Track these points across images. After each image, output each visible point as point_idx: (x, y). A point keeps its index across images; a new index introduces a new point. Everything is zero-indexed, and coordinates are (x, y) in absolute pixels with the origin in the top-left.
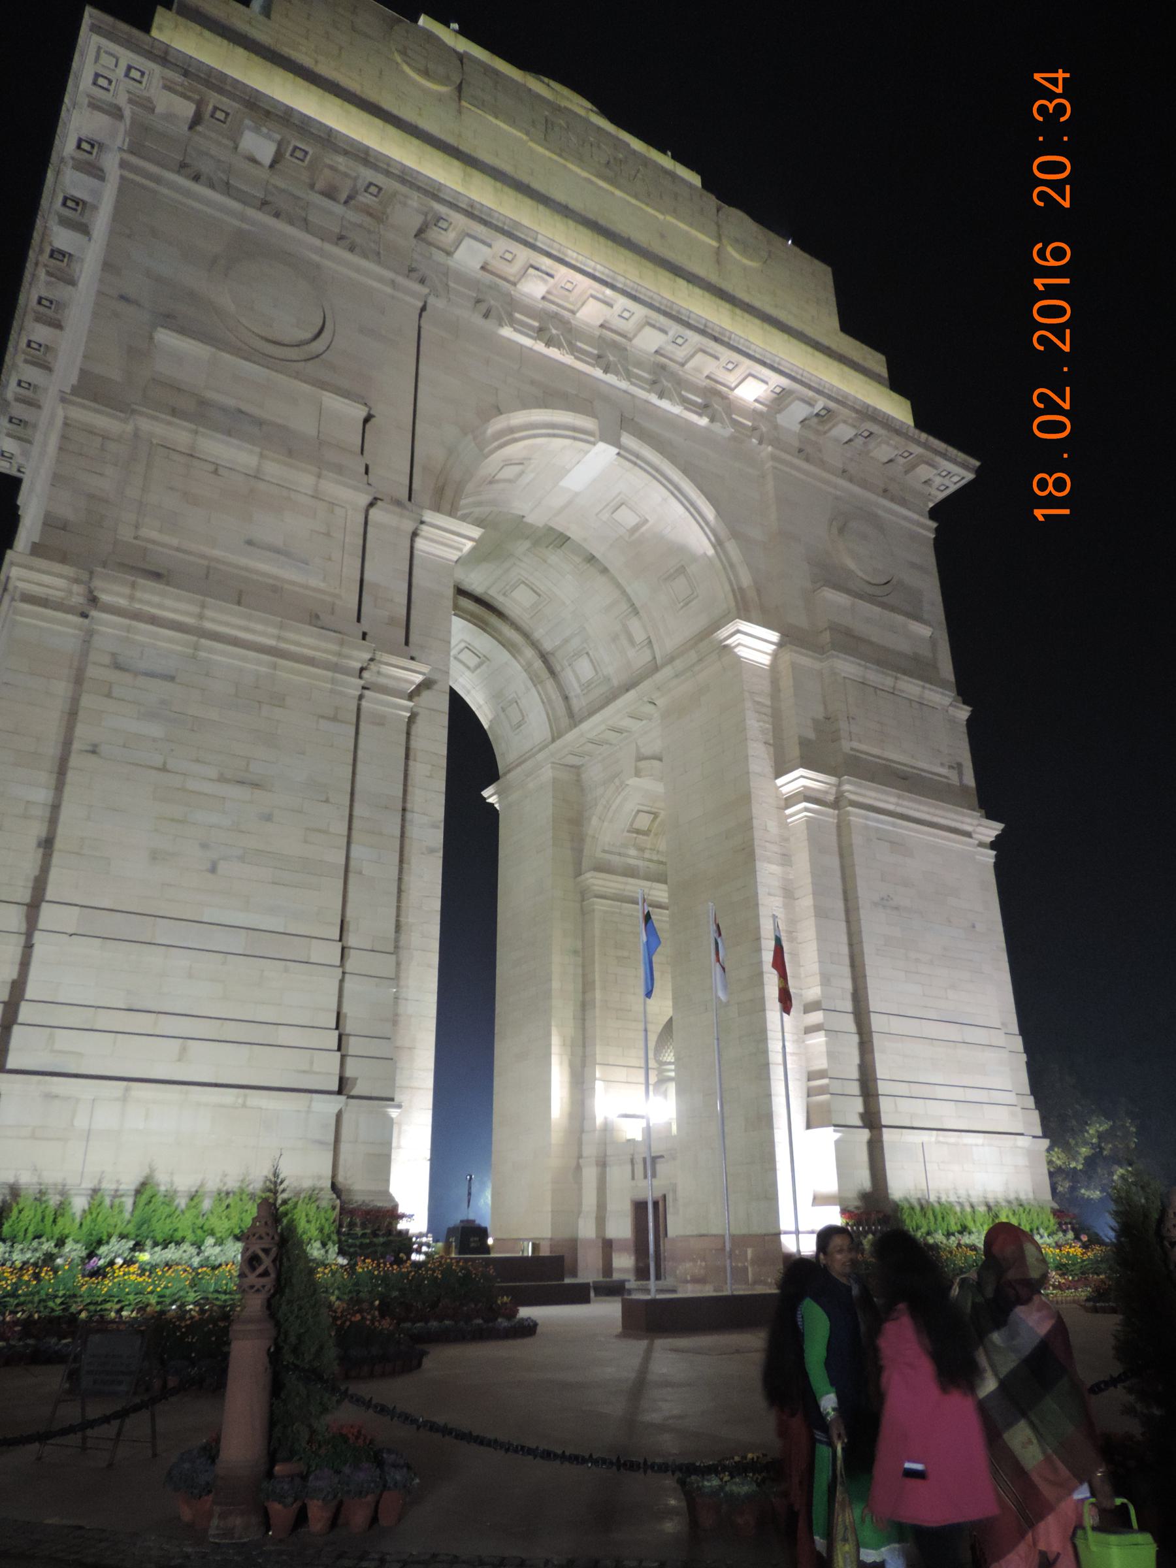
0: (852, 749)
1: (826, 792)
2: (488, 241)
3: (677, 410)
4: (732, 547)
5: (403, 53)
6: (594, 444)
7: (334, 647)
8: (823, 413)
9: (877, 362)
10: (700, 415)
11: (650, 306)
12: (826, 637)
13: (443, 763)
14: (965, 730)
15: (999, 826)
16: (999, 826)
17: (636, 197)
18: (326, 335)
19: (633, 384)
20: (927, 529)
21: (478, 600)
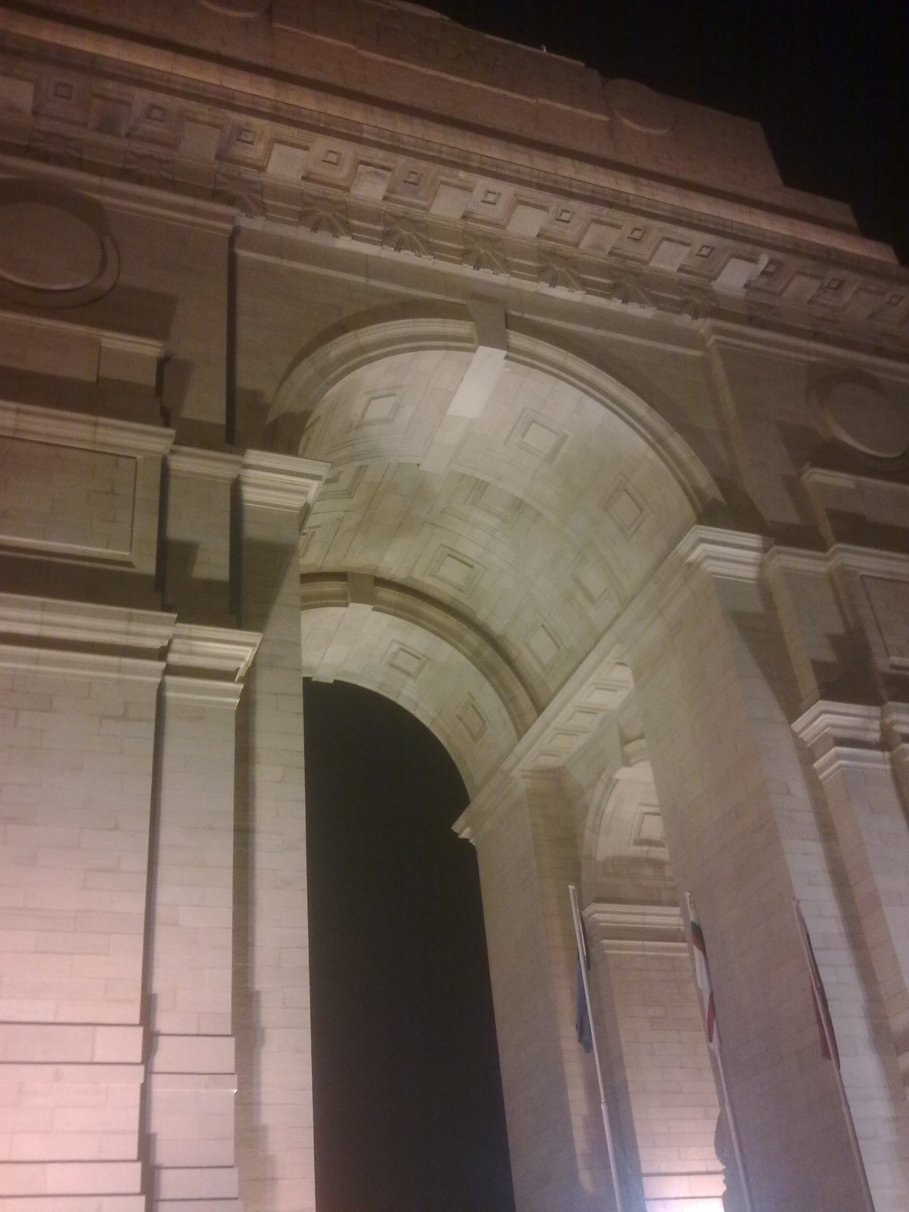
0: (893, 667)
2: (304, 144)
3: (577, 296)
4: (677, 443)
8: (771, 269)
9: (842, 212)
10: (609, 297)
12: (826, 529)
13: (301, 760)
19: (513, 275)
21: (402, 588)
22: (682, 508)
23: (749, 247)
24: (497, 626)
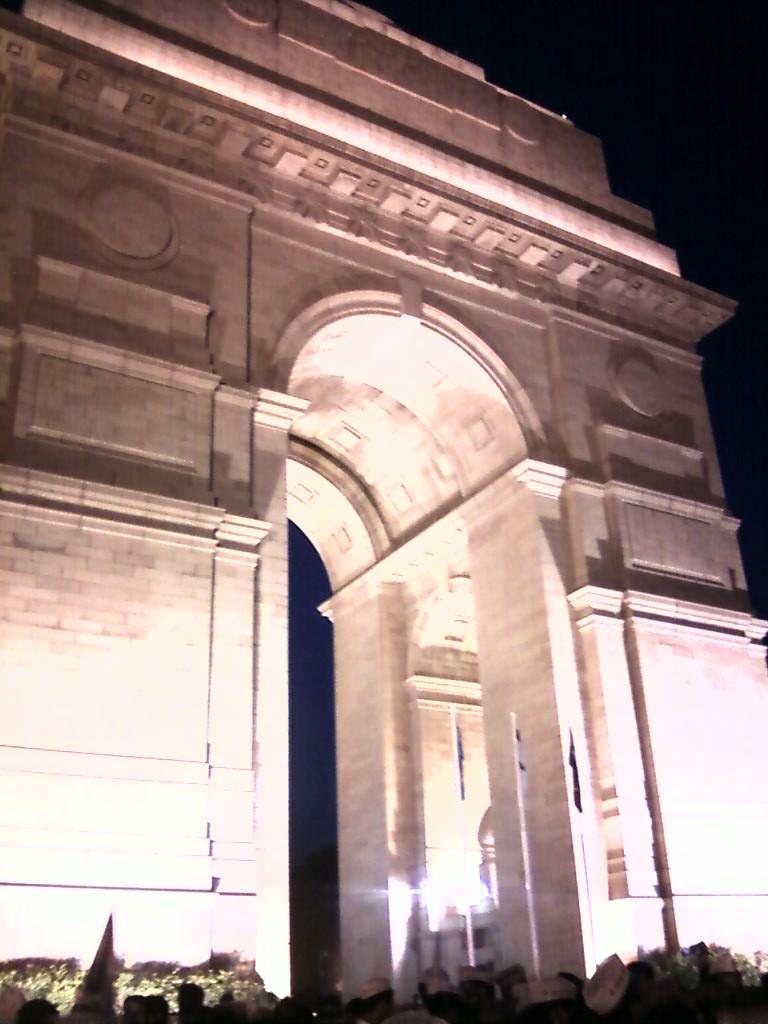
0: (634, 565)
2: (306, 153)
3: (470, 279)
4: (522, 396)
6: (400, 316)
8: (598, 270)
12: (607, 469)
13: (285, 602)
14: (735, 538)
18: (173, 245)
19: (431, 261)
20: (694, 363)
22: (520, 444)
23: (585, 255)
24: (369, 480)
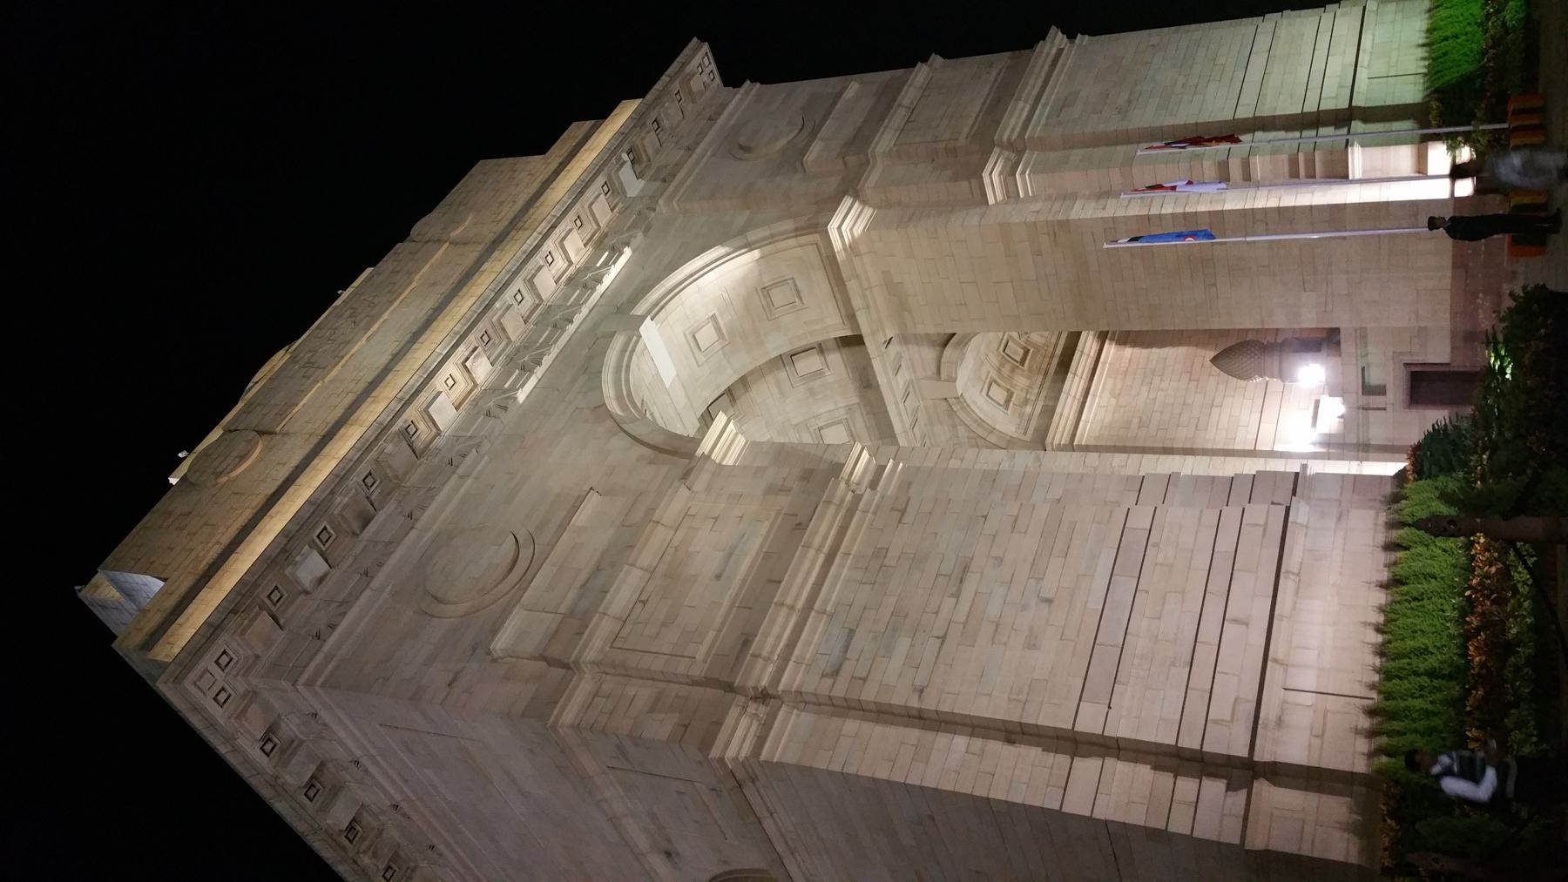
1: (1007, 159)
4: (752, 236)
5: (219, 475)
7: (832, 509)
9: (577, 129)
10: (621, 254)
11: (516, 273)
12: (852, 160)
15: (1053, 29)
16: (1053, 29)
17: (391, 303)
